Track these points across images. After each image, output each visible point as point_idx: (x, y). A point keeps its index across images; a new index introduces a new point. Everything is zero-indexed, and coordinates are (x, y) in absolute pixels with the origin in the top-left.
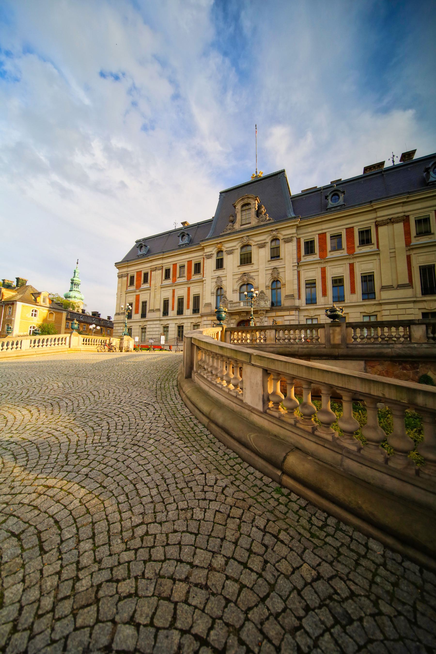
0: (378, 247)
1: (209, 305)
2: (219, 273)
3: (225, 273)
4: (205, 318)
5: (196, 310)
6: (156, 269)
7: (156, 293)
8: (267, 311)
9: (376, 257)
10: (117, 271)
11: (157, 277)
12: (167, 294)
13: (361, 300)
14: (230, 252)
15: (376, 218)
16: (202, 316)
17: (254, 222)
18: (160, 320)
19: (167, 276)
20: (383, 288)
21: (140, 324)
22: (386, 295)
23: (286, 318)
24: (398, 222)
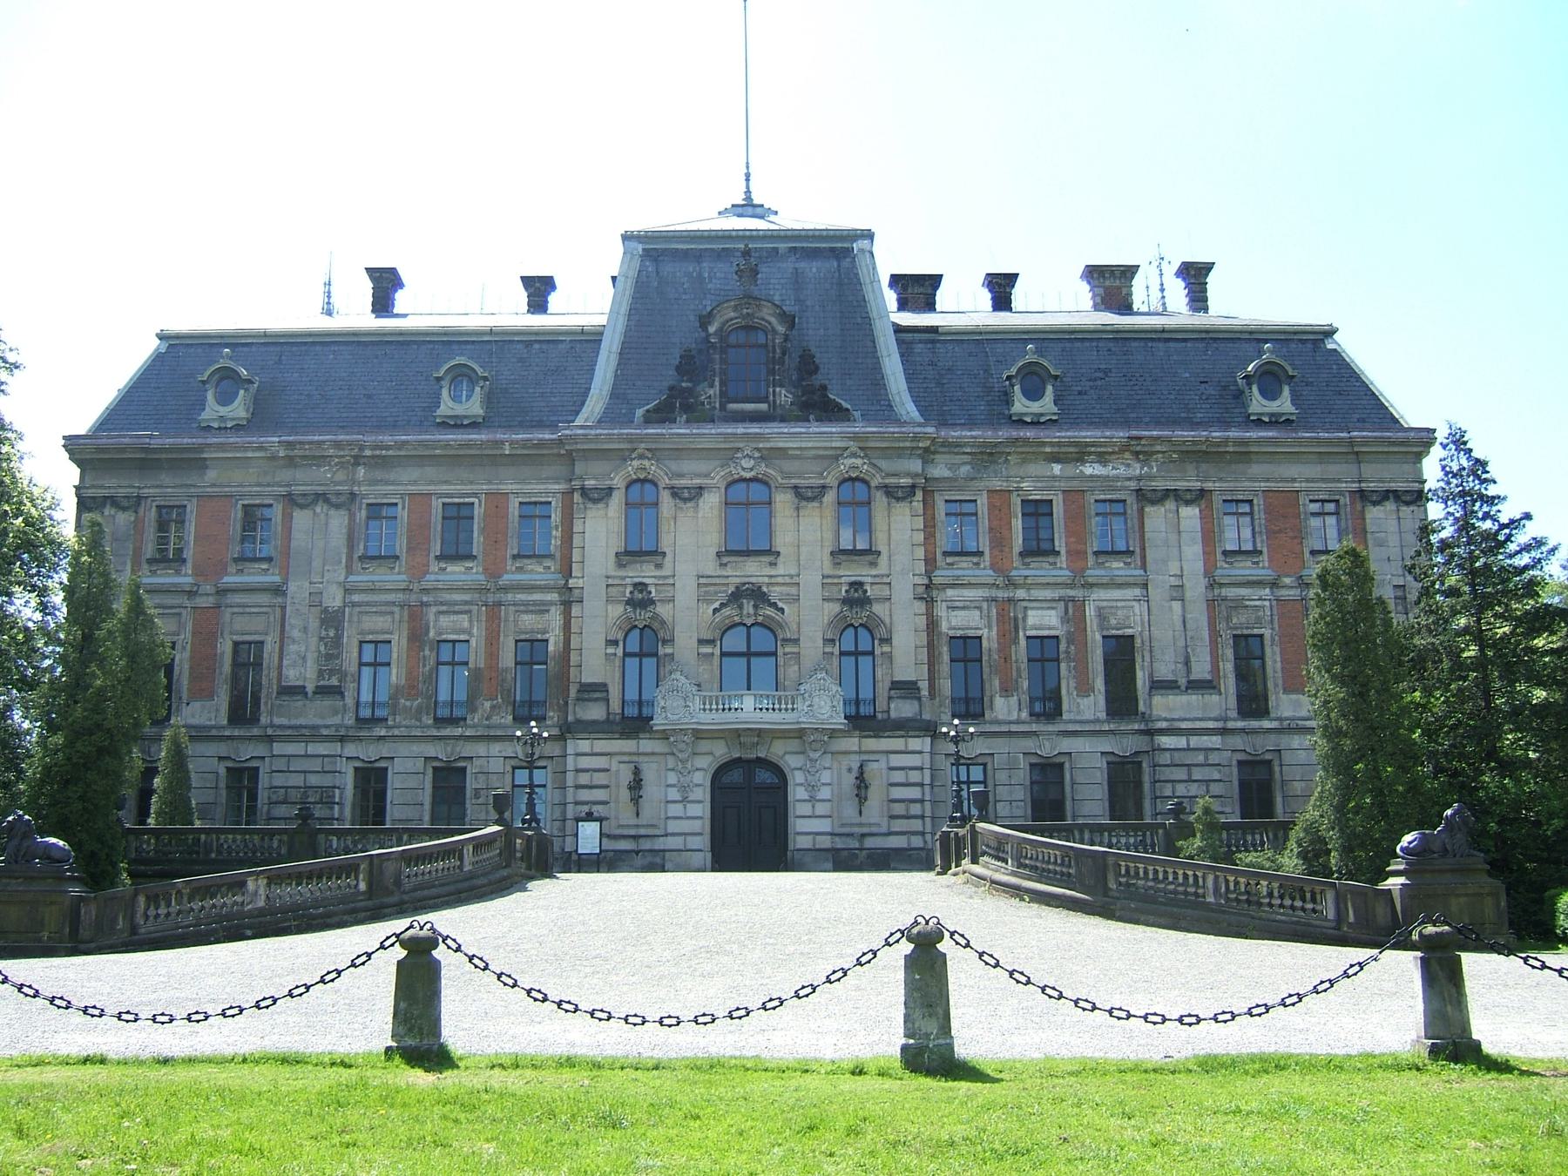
0: (1144, 566)
1: (593, 691)
3: (666, 572)
4: (584, 745)
8: (833, 734)
9: (1137, 592)
10: (75, 472)
13: (1103, 715)
15: (1139, 479)
18: (342, 739)
20: (1158, 686)
21: (223, 749)
22: (1164, 706)
23: (896, 760)
24: (1188, 503)
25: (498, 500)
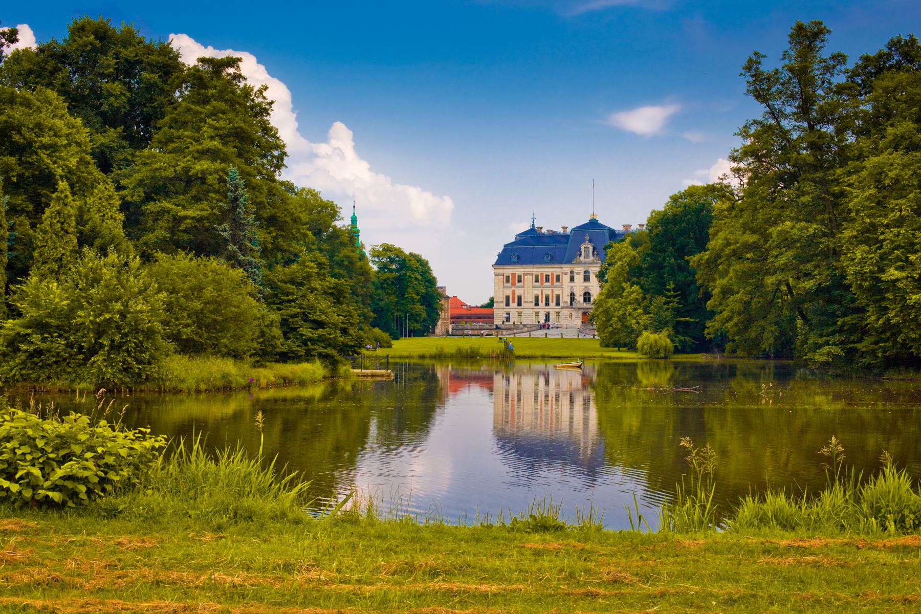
1: (566, 302)
2: (572, 284)
5: (558, 304)
6: (527, 274)
7: (529, 291)
11: (529, 280)
12: (537, 292)
14: (578, 274)
16: (562, 308)
17: (591, 258)
19: (537, 281)
25: (553, 274)
